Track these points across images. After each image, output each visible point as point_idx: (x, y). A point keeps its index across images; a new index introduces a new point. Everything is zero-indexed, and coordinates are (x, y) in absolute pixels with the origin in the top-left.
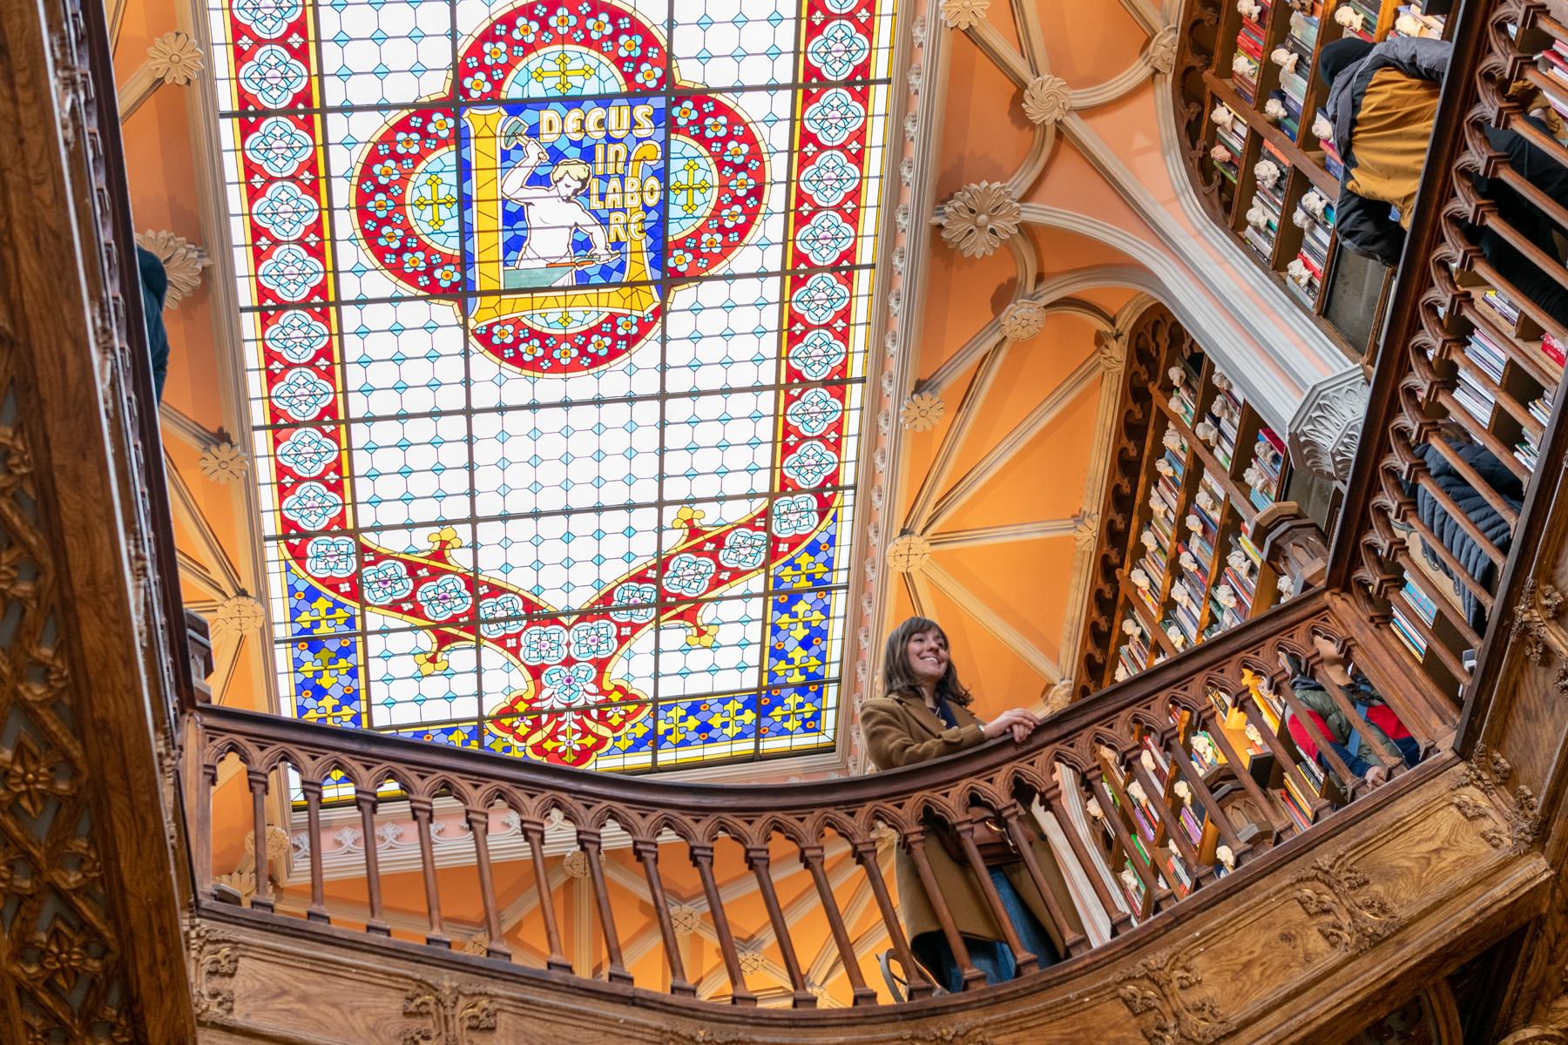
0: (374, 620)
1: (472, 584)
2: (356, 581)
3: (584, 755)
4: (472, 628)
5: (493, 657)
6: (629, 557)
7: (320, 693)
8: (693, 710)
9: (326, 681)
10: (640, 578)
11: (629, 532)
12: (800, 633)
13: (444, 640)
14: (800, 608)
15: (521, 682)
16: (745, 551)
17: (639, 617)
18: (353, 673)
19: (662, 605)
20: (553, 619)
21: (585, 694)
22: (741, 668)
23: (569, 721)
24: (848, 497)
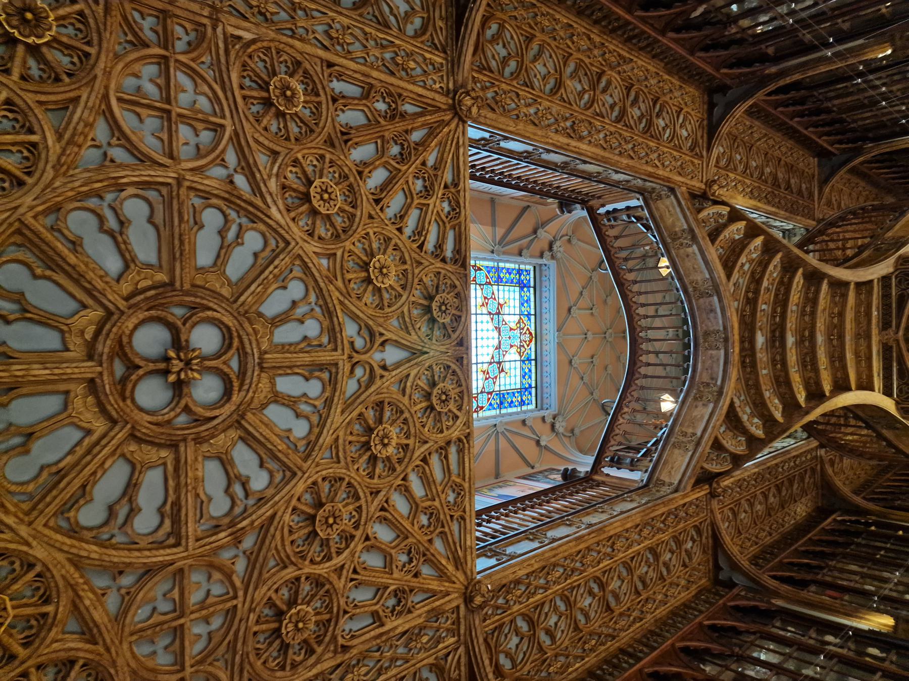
0: (497, 389)
1: (491, 363)
2: (489, 393)
3: (530, 334)
4: (499, 363)
5: (507, 358)
6: (488, 322)
7: (512, 402)
8: (522, 304)
9: (509, 400)
10: (492, 319)
11: (482, 322)
12: (508, 275)
13: (503, 370)
14: (502, 275)
15: (514, 350)
16: (488, 290)
17: (501, 319)
18: (508, 394)
19: (498, 314)
20: (500, 342)
21: (517, 332)
22: (514, 291)
23: (523, 337)
24: (478, 262)
